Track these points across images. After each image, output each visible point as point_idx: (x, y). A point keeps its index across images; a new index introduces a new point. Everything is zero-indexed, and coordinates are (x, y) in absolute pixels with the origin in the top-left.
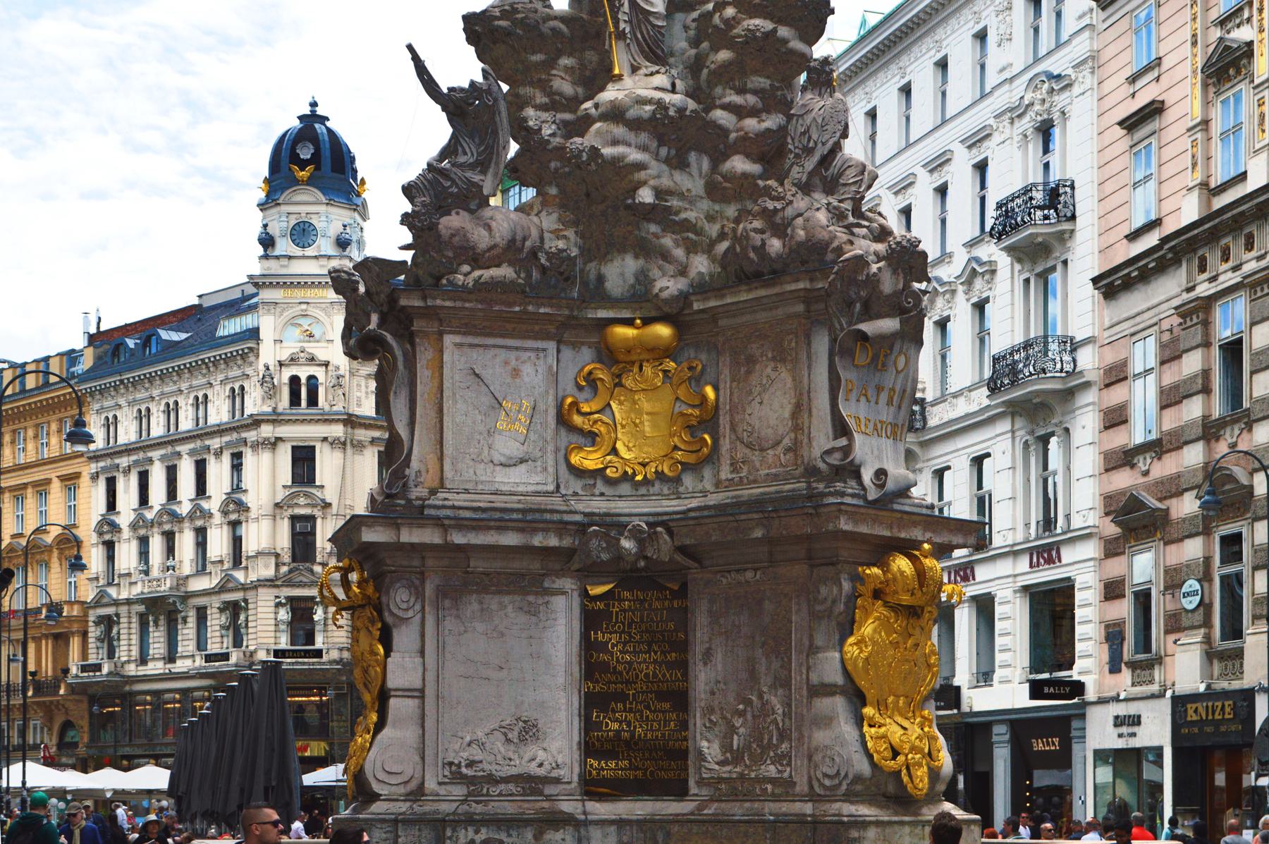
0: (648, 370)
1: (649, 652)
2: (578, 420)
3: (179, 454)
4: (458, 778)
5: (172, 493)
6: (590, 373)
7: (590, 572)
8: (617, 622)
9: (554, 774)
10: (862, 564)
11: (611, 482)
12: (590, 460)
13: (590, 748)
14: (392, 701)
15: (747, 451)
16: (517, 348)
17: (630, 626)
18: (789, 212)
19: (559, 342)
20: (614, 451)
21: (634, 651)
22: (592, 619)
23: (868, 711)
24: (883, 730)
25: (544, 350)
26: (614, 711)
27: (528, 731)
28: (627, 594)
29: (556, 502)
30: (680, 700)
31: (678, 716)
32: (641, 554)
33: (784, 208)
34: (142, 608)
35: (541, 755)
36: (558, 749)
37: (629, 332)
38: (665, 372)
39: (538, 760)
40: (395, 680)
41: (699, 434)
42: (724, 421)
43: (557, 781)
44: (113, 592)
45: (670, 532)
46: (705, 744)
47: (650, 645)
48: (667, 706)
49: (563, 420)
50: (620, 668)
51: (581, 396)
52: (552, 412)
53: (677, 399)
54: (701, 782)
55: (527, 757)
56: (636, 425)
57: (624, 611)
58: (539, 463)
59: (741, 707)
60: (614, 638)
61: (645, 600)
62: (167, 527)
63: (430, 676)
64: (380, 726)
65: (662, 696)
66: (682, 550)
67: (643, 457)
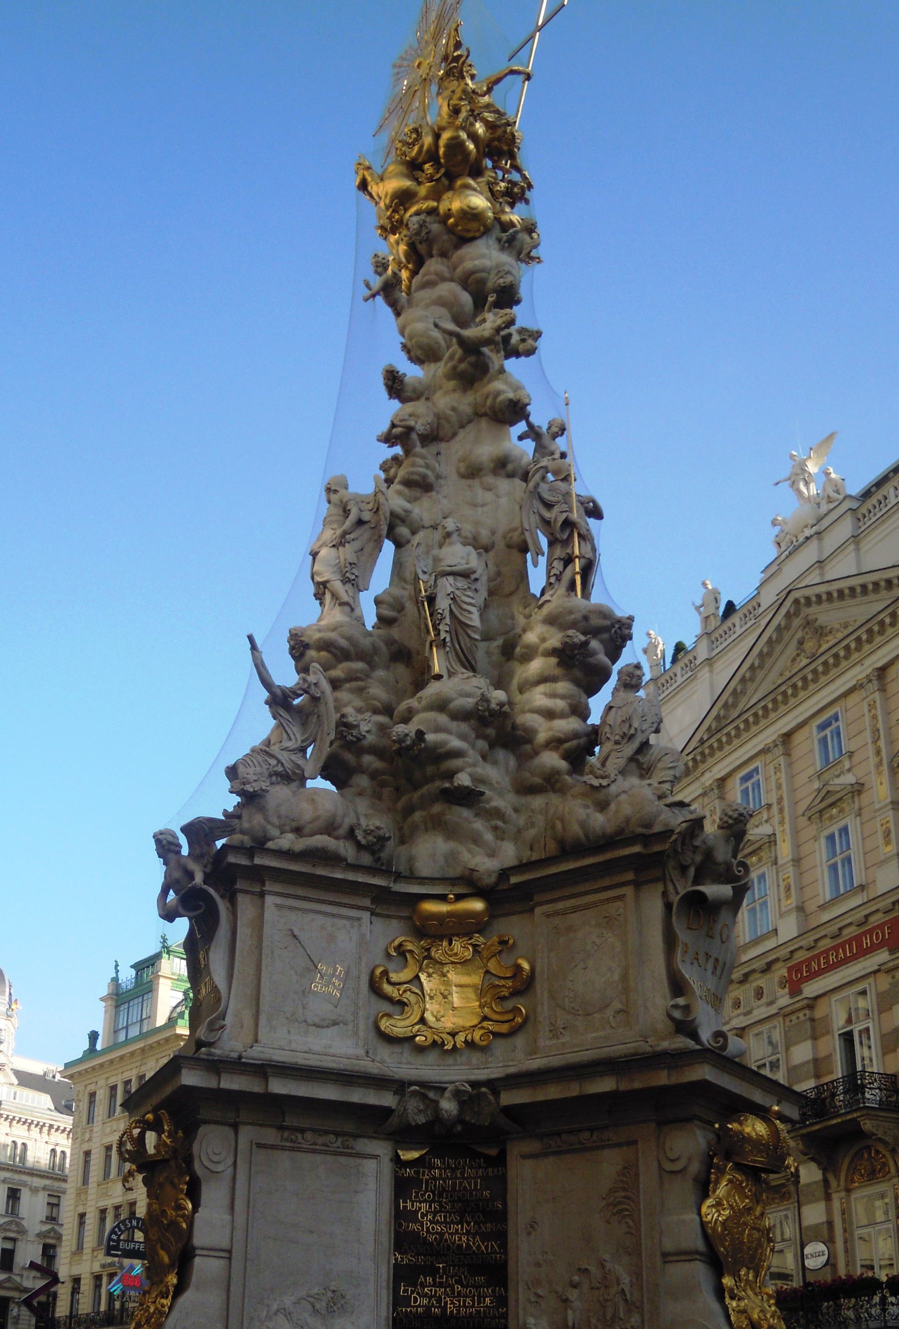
2: (387, 988)
6: (400, 945)
7: (404, 1135)
8: (426, 1191)
11: (421, 1050)
12: (398, 1026)
14: (197, 1260)
15: (569, 1017)
17: (440, 1195)
18: (613, 789)
20: (422, 1021)
21: (445, 1222)
22: (402, 1187)
25: (359, 919)
26: (423, 1286)
28: (438, 1162)
30: (495, 1273)
31: (493, 1291)
33: (609, 785)
38: (475, 946)
40: (198, 1240)
41: (509, 1004)
42: (541, 989)
49: (375, 988)
50: (431, 1238)
51: (391, 967)
52: (365, 979)
53: (487, 972)
56: (445, 997)
57: (435, 1179)
58: (350, 1027)
59: (576, 1278)
60: (424, 1207)
61: (457, 1168)
63: (239, 1235)
66: (509, 1111)
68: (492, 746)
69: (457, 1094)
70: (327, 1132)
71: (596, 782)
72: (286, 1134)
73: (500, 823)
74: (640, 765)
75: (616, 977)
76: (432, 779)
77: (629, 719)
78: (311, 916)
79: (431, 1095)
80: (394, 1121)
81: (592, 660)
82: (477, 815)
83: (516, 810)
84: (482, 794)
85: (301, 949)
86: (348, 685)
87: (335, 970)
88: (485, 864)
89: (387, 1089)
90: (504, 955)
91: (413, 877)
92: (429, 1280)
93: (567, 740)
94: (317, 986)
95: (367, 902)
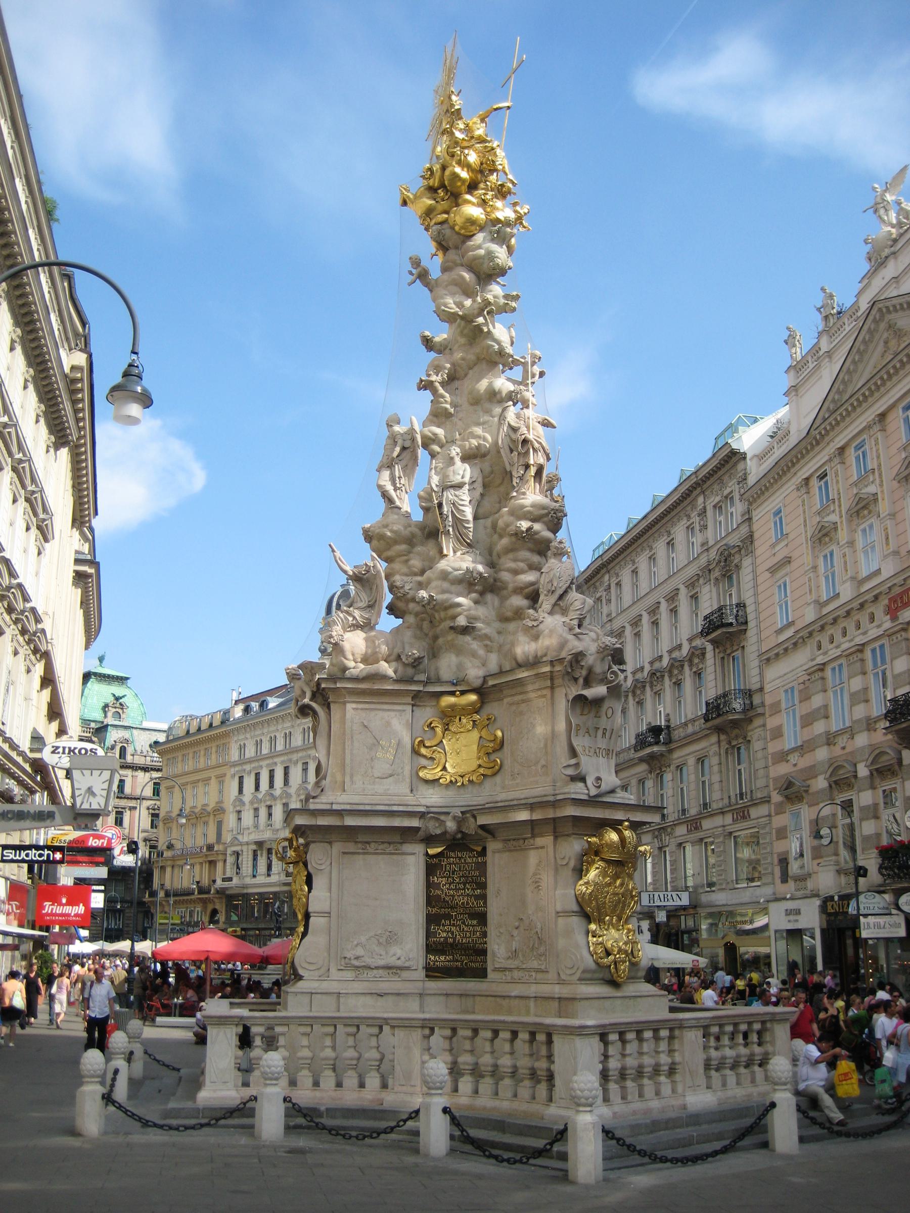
0: (464, 721)
1: (464, 889)
2: (423, 751)
3: (276, 764)
4: (350, 967)
5: (271, 785)
7: (429, 840)
9: (407, 964)
10: (586, 835)
13: (431, 948)
16: (389, 710)
17: (453, 874)
19: (413, 705)
20: (444, 769)
21: (456, 889)
22: (431, 868)
23: (593, 927)
24: (601, 939)
27: (391, 938)
28: (452, 854)
29: (410, 799)
30: (482, 918)
32: (459, 831)
34: (254, 847)
35: (399, 952)
36: (411, 948)
37: (452, 700)
39: (398, 956)
43: (407, 968)
44: (240, 837)
45: (474, 817)
46: (496, 947)
47: (465, 885)
48: (475, 922)
49: (415, 752)
54: (496, 970)
55: (391, 953)
57: (450, 864)
60: (444, 881)
62: (268, 803)
64: (305, 934)
65: (472, 916)
66: (482, 827)
67: (461, 771)
68: (482, 594)
69: (454, 818)
70: (383, 843)
71: (530, 624)
72: (360, 845)
73: (489, 643)
74: (561, 608)
75: (542, 745)
76: (445, 619)
77: (551, 581)
78: (373, 713)
79: (442, 818)
80: (421, 833)
81: (536, 536)
82: (474, 639)
83: (499, 633)
84: (473, 628)
85: (369, 734)
86: (398, 559)
87: (391, 743)
88: (474, 673)
89: (415, 816)
90: (490, 727)
91: (439, 681)
92: (448, 922)
93: (526, 587)
94: (379, 754)
95: (409, 700)
